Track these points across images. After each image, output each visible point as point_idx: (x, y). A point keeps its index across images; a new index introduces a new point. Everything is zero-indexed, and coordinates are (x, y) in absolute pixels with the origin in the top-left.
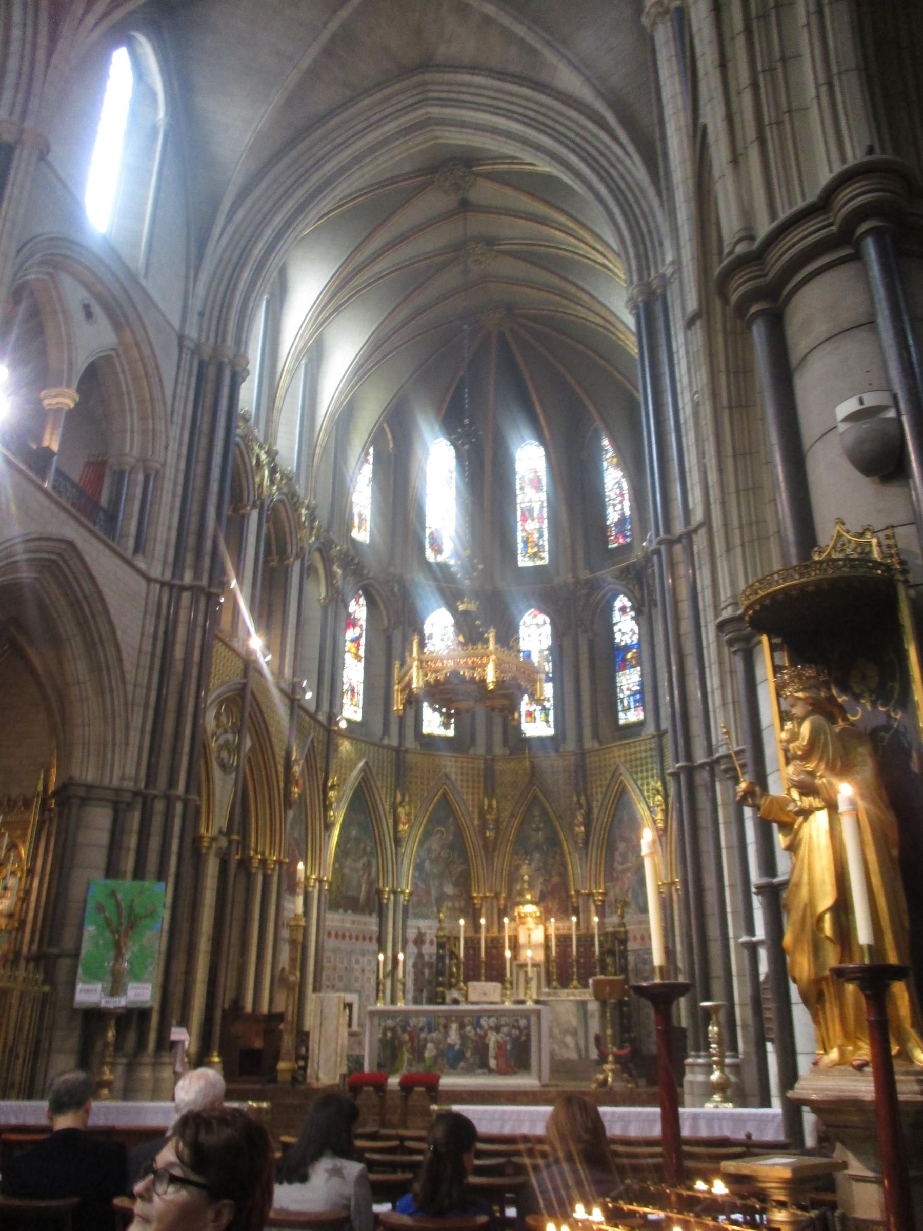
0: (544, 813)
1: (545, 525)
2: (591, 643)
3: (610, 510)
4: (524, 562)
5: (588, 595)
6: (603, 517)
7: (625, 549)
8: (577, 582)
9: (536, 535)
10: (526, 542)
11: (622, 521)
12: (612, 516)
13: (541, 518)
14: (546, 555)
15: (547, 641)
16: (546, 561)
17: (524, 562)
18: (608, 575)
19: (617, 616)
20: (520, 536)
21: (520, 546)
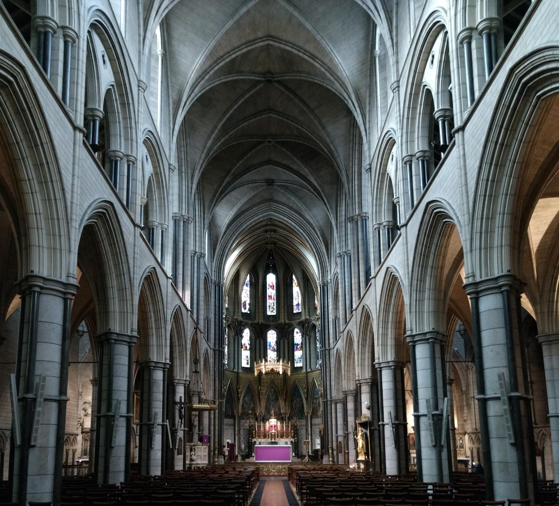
0: (275, 390)
1: (275, 302)
2: (288, 342)
3: (294, 300)
4: (269, 313)
5: (288, 328)
6: (292, 302)
7: (299, 314)
8: (285, 323)
9: (273, 305)
10: (269, 307)
11: (298, 305)
12: (295, 302)
13: (274, 299)
14: (275, 311)
15: (275, 340)
16: (275, 314)
17: (269, 313)
18: (294, 323)
19: (295, 334)
20: (268, 304)
21: (268, 308)
